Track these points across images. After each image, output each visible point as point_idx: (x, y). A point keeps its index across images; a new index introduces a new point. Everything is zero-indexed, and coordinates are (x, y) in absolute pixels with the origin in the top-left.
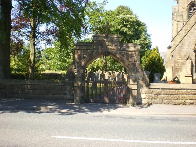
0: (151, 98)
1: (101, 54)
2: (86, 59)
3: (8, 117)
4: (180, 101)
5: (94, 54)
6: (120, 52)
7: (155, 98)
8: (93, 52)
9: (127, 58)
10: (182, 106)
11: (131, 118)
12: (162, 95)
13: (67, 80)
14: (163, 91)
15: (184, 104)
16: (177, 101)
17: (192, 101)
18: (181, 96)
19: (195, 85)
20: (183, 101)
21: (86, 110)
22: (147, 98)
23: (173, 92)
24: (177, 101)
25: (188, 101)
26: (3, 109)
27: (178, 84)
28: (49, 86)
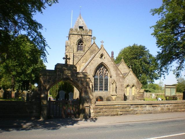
0: (97, 112)
1: (62, 79)
2: (50, 83)
3: (5, 135)
4: (115, 113)
5: (57, 79)
6: (76, 78)
7: (99, 112)
8: (56, 78)
9: (81, 83)
10: (116, 116)
11: (83, 128)
12: (104, 110)
13: (34, 100)
14: (104, 107)
15: (117, 115)
16: (112, 113)
17: (121, 113)
18: (115, 109)
19: (184, 101)
20: (116, 113)
21: (2, 131)
22: (94, 112)
23: (110, 107)
24: (112, 113)
25: (119, 113)
26: (6, 127)
27: (109, 102)
28: (17, 106)
